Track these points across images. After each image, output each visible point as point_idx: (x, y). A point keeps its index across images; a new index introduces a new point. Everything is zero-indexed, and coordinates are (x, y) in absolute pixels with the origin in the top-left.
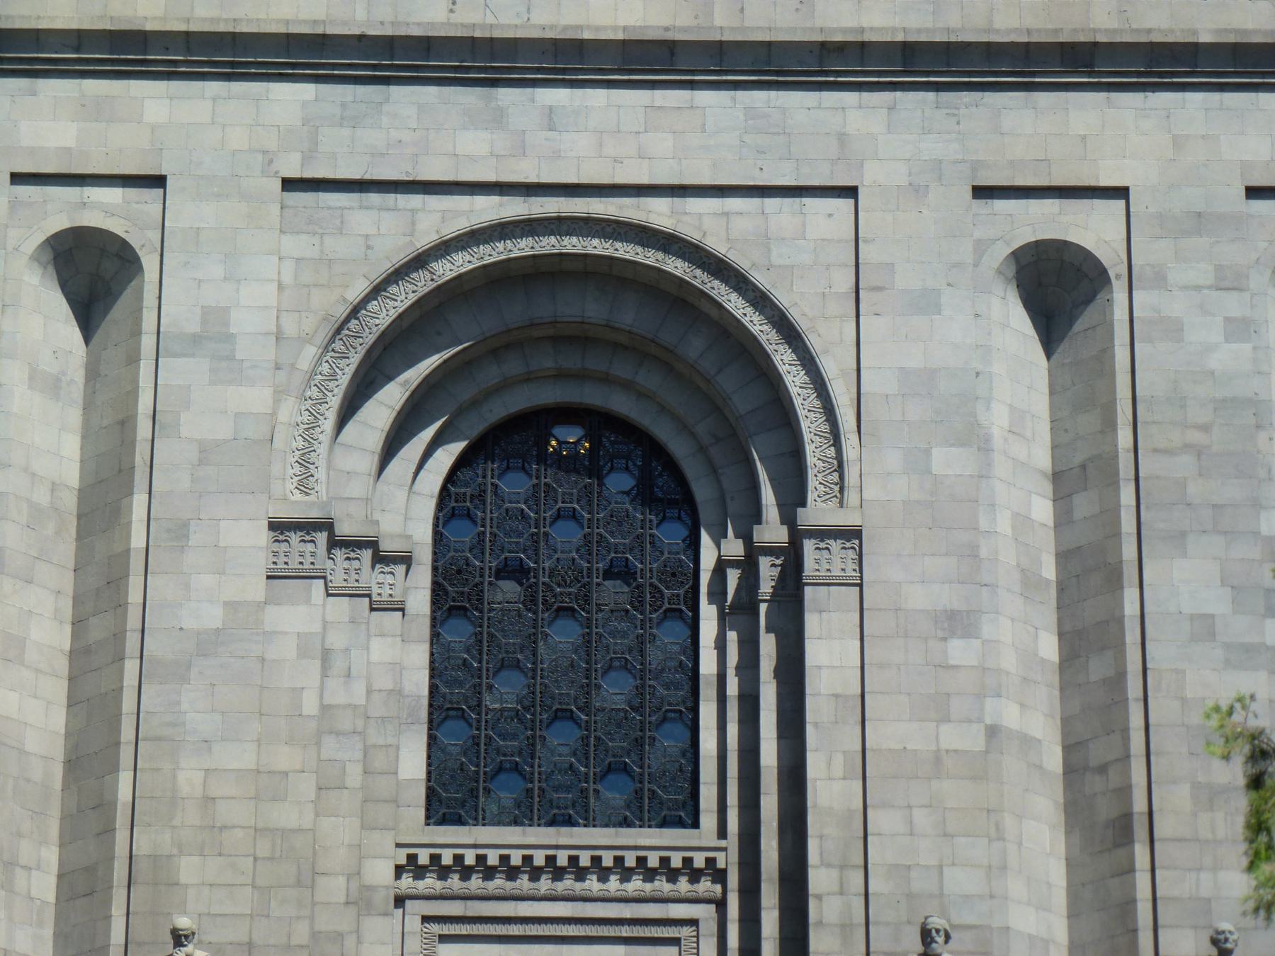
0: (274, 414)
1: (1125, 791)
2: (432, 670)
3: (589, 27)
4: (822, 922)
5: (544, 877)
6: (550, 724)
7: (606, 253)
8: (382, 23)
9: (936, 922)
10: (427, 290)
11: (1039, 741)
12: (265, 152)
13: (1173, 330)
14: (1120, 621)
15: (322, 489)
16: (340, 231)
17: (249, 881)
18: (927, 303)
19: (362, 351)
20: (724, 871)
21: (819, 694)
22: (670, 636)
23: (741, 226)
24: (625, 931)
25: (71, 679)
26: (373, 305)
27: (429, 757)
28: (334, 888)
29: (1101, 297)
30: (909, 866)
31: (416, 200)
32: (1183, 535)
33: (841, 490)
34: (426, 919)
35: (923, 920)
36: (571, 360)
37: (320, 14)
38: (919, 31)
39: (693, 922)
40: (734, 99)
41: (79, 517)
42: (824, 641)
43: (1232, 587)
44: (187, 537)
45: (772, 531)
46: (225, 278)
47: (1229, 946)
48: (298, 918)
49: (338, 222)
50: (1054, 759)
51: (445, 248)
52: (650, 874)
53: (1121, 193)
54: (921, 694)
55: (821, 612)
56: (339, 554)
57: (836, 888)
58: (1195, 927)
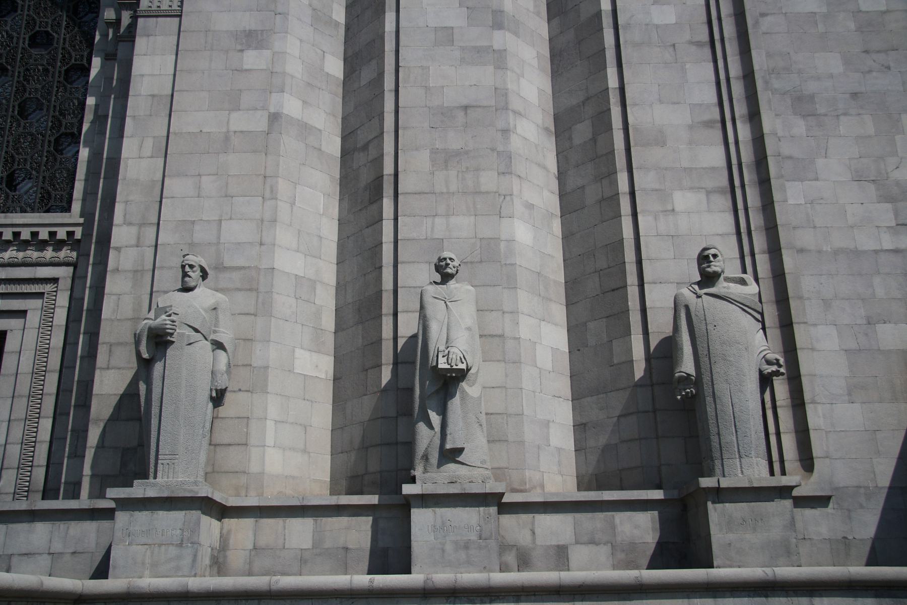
1: (379, 160)
4: (118, 270)
11: (320, 130)
21: (140, 95)
30: (194, 221)
35: (183, 259)
39: (55, 280)
42: (149, 57)
47: (449, 270)
50: (333, 145)
52: (24, 245)
54: (219, 91)
55: (148, 36)
57: (133, 242)
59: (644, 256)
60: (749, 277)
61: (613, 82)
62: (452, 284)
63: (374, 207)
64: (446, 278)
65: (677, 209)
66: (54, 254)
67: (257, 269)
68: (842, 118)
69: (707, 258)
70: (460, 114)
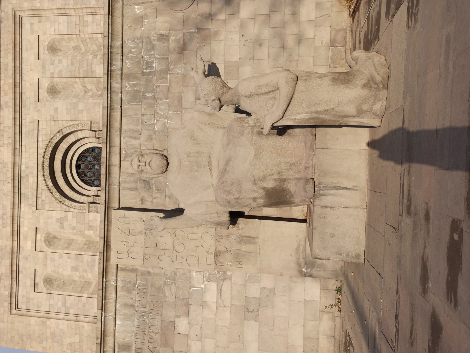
3: (12, 162)
7: (49, 160)
8: (11, 194)
12: (32, 212)
13: (60, 71)
18: (56, 110)
23: (44, 139)
26: (56, 196)
32: (92, 71)
37: (10, 203)
40: (24, 139)
43: (100, 64)
44: (91, 225)
46: (52, 219)
49: (43, 201)
51: (47, 185)
53: (39, 78)
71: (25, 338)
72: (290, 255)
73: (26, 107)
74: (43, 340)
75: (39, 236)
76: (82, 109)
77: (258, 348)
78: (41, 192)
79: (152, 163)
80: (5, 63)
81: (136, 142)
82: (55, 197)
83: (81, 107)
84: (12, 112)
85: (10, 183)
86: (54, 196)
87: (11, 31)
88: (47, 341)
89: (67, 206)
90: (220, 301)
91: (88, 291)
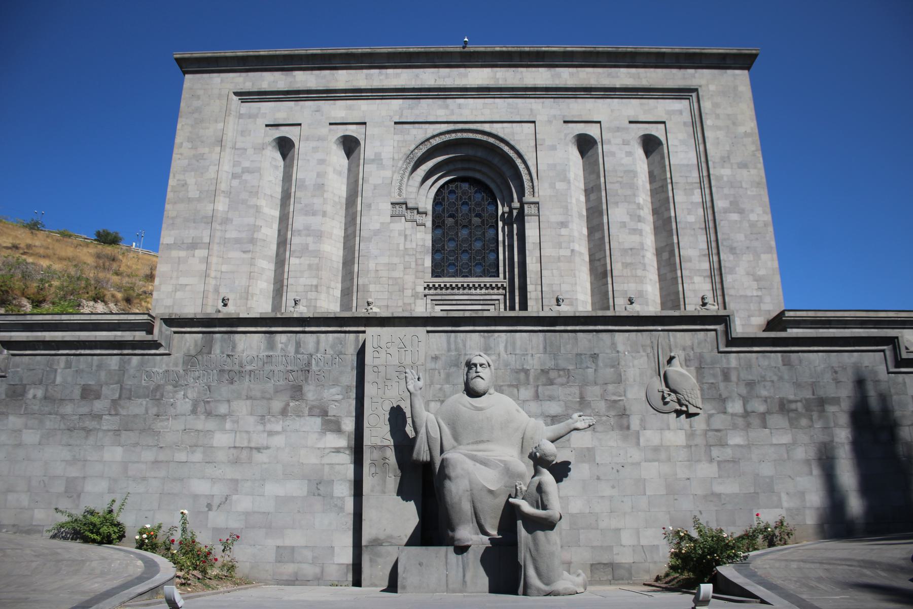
0: (392, 177)
1: (605, 265)
2: (432, 241)
5: (461, 289)
6: (462, 253)
9: (560, 297)
10: (429, 147)
12: (390, 116)
13: (613, 154)
14: (603, 224)
15: (404, 196)
16: (408, 134)
17: (387, 290)
18: (553, 148)
19: (414, 162)
20: (506, 288)
22: (491, 232)
24: (481, 302)
25: (344, 243)
26: (416, 151)
27: (432, 261)
28: (408, 293)
29: (595, 147)
31: (427, 126)
32: (617, 203)
33: (534, 193)
34: (432, 300)
36: (466, 165)
37: (404, 84)
38: (549, 85)
39: (499, 300)
40: (504, 101)
41: (346, 204)
43: (630, 215)
45: (516, 204)
46: (381, 146)
47: (633, 301)
48: (399, 299)
50: (587, 258)
51: (433, 137)
52: (487, 288)
53: (599, 122)
56: (409, 211)
57: (534, 290)
58: (624, 298)
59: (685, 296)
60: (716, 304)
61: (675, 241)
62: (634, 304)
63: (604, 280)
64: (632, 303)
65: (695, 282)
66: (498, 291)
67: (573, 299)
68: (744, 255)
69: (704, 298)
70: (630, 251)
71: (196, 115)
72: (385, 530)
73: (554, 102)
74: (192, 142)
75: (354, 127)
76: (557, 188)
77: (278, 496)
78: (422, 128)
79: (479, 379)
80: (619, 74)
81: (501, 348)
82: (415, 149)
83: (560, 186)
84: (546, 85)
85: (436, 83)
86: (417, 147)
87: (668, 84)
88: (192, 148)
89: (401, 167)
90: (327, 451)
91: (266, 207)
